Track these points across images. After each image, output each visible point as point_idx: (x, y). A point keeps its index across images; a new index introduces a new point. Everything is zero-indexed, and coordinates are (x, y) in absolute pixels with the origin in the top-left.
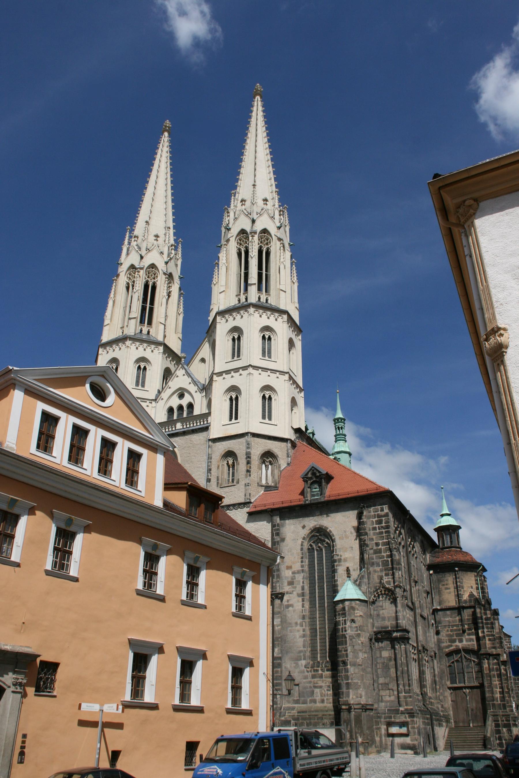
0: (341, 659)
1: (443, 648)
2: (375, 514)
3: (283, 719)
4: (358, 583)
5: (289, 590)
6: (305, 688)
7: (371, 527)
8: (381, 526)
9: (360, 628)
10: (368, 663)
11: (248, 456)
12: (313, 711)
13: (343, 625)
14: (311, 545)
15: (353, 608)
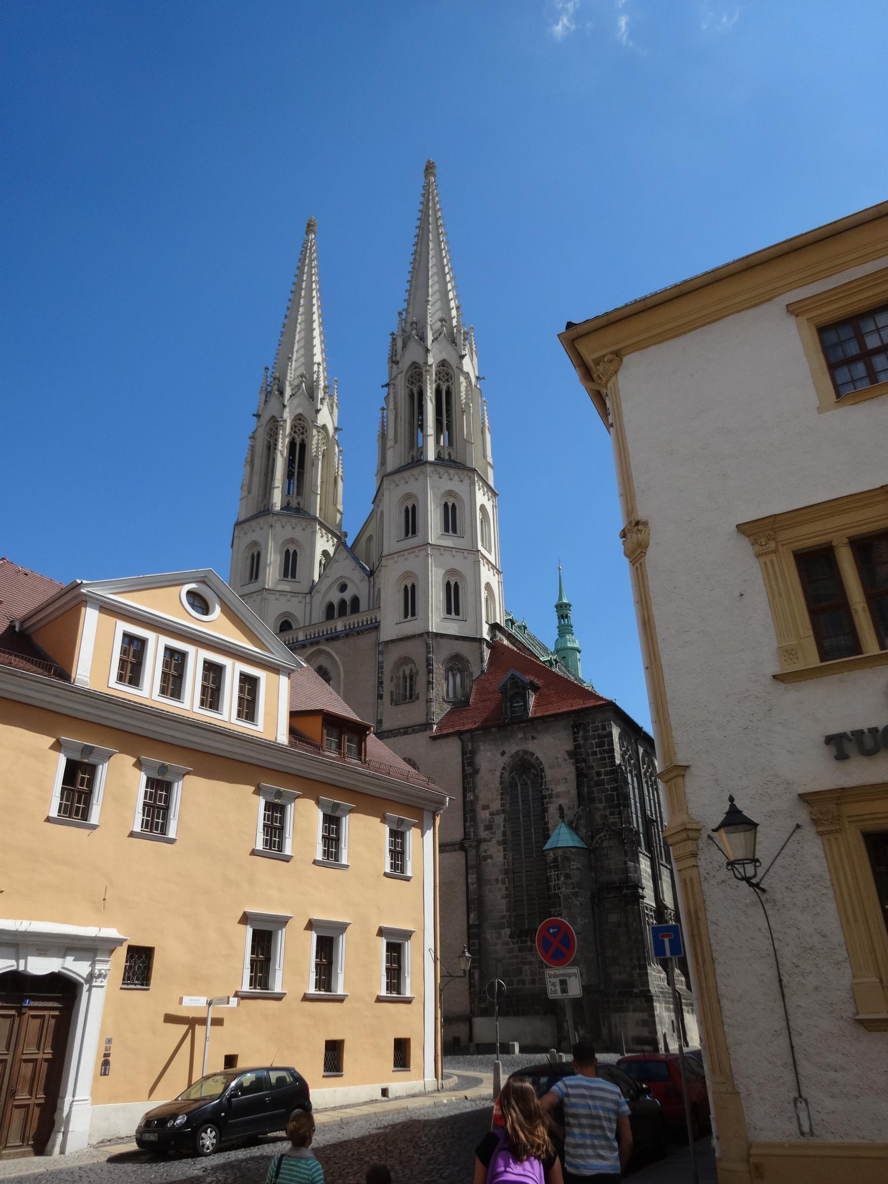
2: (595, 734)
3: (483, 1006)
4: (573, 827)
7: (590, 751)
11: (429, 663)
13: (555, 881)
15: (568, 859)
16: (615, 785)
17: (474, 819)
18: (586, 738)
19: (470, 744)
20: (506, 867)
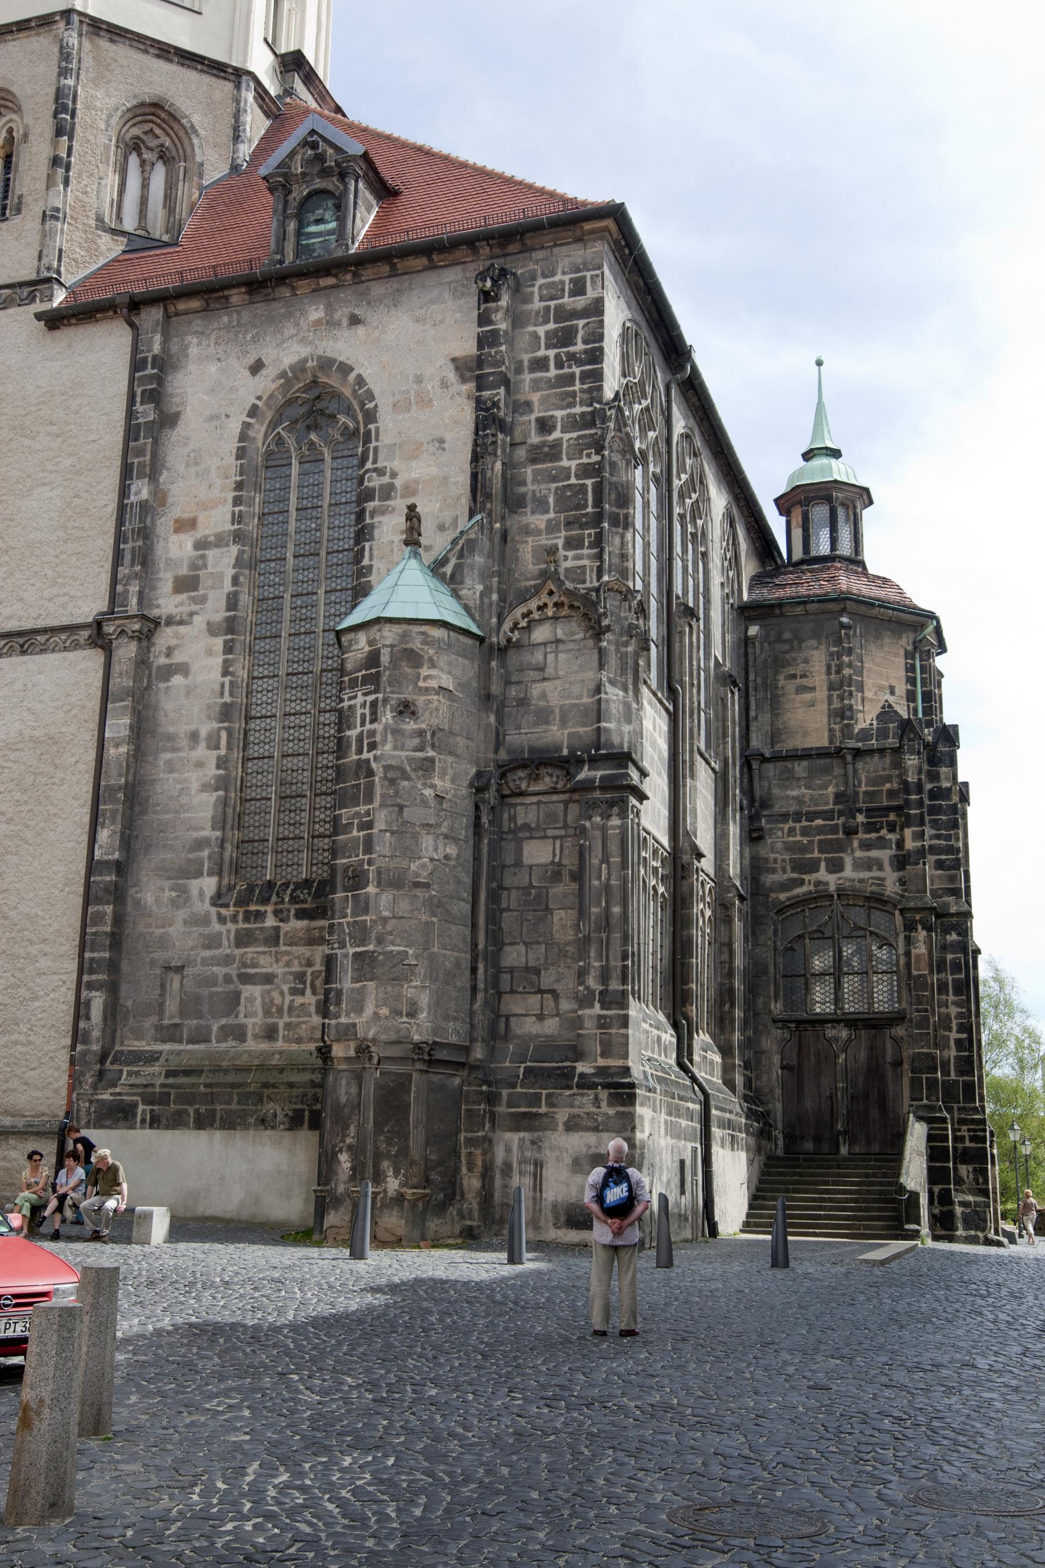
0: (344, 861)
1: (771, 890)
3: (106, 1096)
5: (180, 609)
6: (209, 981)
7: (526, 358)
8: (568, 354)
9: (435, 738)
10: (459, 882)
12: (226, 1071)
13: (363, 724)
14: (279, 441)
15: (414, 658)
16: (596, 458)
17: (145, 559)
18: (517, 320)
19: (158, 338)
20: (227, 699)
